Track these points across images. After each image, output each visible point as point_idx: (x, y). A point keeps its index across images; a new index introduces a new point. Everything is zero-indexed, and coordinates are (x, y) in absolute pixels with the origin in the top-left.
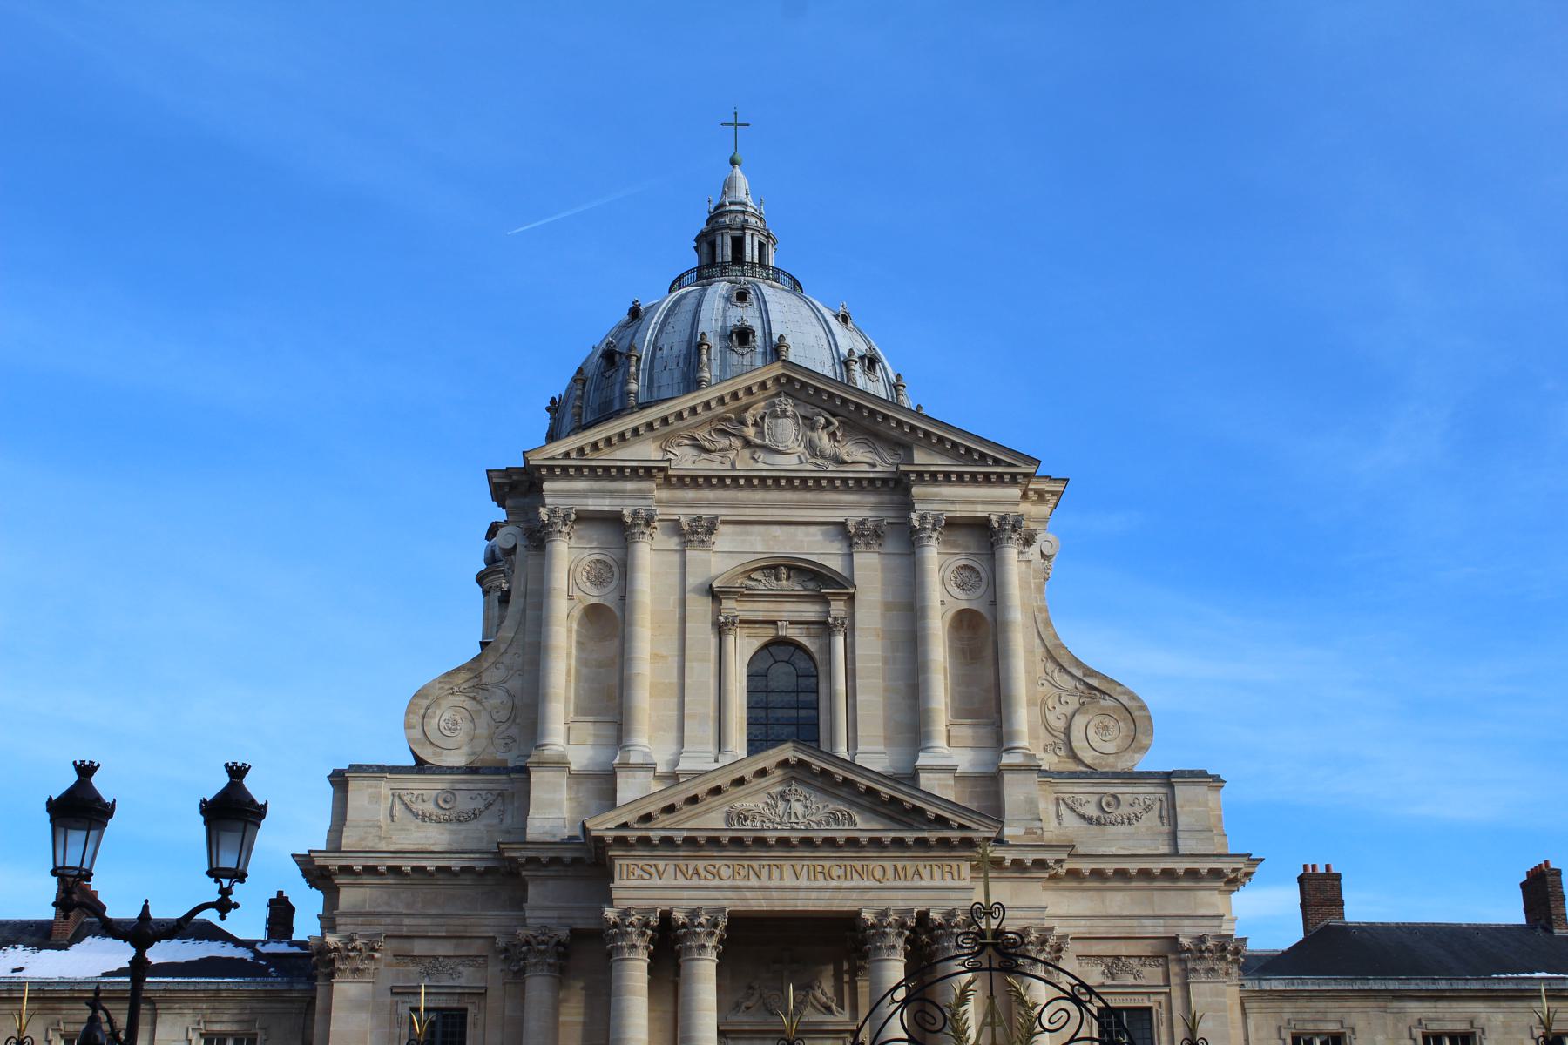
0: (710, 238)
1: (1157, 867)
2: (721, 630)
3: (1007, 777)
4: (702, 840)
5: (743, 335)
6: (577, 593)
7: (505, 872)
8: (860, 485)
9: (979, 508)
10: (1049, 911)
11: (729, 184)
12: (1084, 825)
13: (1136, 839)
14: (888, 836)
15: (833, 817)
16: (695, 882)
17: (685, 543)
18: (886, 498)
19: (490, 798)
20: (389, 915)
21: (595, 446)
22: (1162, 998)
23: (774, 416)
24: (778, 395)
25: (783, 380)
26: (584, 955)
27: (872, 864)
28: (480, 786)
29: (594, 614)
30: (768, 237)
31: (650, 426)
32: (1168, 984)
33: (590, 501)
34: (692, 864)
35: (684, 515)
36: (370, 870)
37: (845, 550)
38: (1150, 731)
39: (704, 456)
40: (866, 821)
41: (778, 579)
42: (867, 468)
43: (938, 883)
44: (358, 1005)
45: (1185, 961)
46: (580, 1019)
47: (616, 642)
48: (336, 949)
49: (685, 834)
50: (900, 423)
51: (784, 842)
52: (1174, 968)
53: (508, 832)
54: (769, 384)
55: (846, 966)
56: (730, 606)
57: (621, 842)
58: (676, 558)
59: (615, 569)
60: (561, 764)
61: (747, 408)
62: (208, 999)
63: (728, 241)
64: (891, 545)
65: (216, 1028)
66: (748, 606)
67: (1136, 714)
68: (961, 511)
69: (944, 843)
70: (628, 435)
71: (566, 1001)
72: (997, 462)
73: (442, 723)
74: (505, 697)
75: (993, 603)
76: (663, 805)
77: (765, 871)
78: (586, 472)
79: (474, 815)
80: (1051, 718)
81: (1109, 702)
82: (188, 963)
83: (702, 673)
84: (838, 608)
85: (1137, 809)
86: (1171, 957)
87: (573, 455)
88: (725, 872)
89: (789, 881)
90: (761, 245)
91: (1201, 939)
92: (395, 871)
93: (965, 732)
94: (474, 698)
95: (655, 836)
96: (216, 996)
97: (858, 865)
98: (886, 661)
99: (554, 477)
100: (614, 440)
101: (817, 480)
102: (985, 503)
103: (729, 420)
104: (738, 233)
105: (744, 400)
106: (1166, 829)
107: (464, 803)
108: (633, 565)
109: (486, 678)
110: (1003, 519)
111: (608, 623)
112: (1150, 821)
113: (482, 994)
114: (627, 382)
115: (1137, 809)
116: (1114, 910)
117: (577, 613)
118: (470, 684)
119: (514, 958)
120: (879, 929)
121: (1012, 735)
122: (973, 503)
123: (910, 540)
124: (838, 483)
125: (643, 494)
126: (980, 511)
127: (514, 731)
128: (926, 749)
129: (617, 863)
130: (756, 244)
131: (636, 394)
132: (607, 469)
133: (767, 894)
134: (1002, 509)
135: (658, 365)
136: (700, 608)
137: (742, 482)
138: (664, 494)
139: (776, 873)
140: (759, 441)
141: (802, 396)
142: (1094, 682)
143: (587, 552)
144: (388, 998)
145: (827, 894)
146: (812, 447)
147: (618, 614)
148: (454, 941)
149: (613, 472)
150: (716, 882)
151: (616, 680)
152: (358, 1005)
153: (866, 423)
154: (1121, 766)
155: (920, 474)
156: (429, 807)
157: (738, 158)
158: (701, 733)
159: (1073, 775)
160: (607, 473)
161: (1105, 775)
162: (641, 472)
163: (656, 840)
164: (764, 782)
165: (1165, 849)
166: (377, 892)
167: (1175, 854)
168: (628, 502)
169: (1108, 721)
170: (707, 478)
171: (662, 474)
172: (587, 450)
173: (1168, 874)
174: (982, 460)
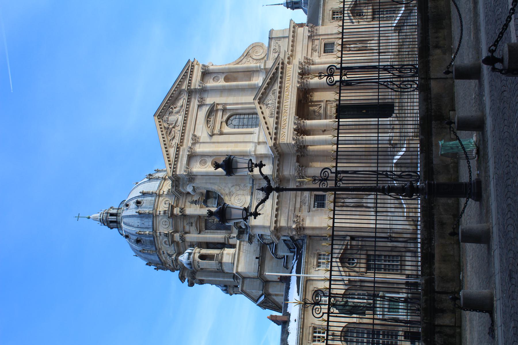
0: (109, 222)
2: (221, 134)
3: (267, 67)
5: (138, 203)
8: (189, 101)
11: (95, 219)
13: (284, 45)
14: (279, 80)
15: (273, 93)
16: (287, 125)
17: (198, 142)
18: (193, 96)
21: (169, 161)
30: (111, 208)
31: (166, 148)
32: (319, 39)
34: (282, 125)
36: (276, 216)
44: (312, 220)
45: (314, 36)
46: (319, 163)
50: (174, 91)
52: (315, 38)
56: (216, 131)
57: (275, 139)
58: (202, 145)
61: (165, 127)
64: (205, 96)
65: (315, 263)
66: (216, 128)
69: (282, 68)
72: (188, 69)
75: (223, 73)
81: (251, 52)
83: (232, 138)
84: (220, 107)
85: (277, 45)
88: (285, 118)
89: (289, 103)
91: (309, 31)
92: (277, 210)
93: (254, 79)
95: (274, 131)
96: (307, 263)
101: (186, 111)
102: (198, 73)
103: (167, 132)
104: (109, 214)
108: (202, 152)
109: (228, 192)
110: (202, 69)
112: (280, 43)
114: (146, 234)
121: (257, 67)
123: (203, 91)
125: (184, 150)
126: (200, 74)
127: (242, 185)
132: (176, 158)
134: (200, 68)
135: (143, 226)
136: (215, 138)
138: (184, 146)
141: (164, 114)
144: (311, 213)
145: (293, 95)
147: (214, 157)
152: (312, 220)
153: (173, 99)
154: (266, 49)
155: (188, 86)
157: (88, 216)
158: (247, 138)
159: (267, 58)
166: (282, 217)
170: (182, 136)
171: (179, 146)
173: (293, 37)
174: (188, 69)
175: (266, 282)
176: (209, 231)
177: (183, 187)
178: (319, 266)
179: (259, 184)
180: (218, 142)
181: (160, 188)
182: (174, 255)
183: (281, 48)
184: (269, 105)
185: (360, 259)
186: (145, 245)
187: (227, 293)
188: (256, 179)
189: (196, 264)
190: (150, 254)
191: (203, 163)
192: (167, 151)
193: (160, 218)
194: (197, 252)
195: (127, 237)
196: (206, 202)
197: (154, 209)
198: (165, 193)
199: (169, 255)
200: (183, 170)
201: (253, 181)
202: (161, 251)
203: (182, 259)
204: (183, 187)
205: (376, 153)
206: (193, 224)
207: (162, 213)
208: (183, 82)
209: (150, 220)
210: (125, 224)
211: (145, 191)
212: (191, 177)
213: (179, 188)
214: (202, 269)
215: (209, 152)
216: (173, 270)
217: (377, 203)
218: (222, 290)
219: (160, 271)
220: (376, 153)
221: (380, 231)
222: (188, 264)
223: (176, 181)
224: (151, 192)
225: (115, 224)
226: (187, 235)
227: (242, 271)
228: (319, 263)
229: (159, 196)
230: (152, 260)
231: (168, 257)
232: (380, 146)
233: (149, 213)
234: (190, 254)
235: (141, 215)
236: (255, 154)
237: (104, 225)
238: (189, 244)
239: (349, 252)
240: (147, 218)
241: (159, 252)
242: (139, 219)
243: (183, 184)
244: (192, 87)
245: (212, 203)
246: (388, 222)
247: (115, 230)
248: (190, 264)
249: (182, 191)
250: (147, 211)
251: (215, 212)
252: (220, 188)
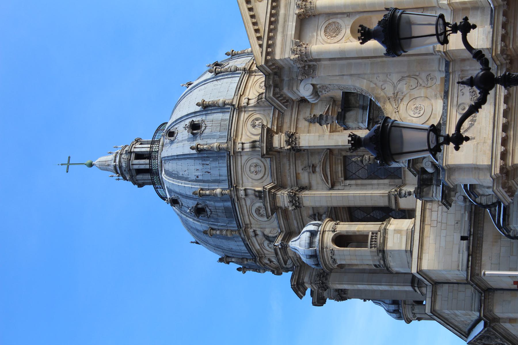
0: (134, 173)
5: (195, 127)
11: (104, 167)
21: (257, 31)
28: (456, 91)
30: (137, 141)
33: (289, 33)
36: (505, 142)
59: (331, 21)
63: (136, 162)
70: (252, 13)
73: (416, 115)
74: (404, 82)
78: (271, 34)
87: (261, 42)
90: (141, 144)
92: (505, 128)
94: (402, 100)
100: (254, 20)
104: (133, 156)
108: (330, 7)
109: (391, 94)
114: (215, 195)
127: (424, 75)
130: (141, 146)
131: (223, 189)
132: (271, 23)
135: (207, 177)
143: (319, 38)
157: (88, 162)
160: (273, 23)
168: (291, 12)
172: (258, 35)
175: (486, 292)
176: (353, 182)
177: (290, 88)
179: (462, 71)
181: (241, 91)
182: (280, 239)
186: (216, 219)
187: (400, 318)
188: (454, 61)
189: (327, 255)
190: (226, 238)
191: (333, 30)
192: (250, 9)
193: (244, 158)
194: (329, 229)
195: (174, 202)
196: (344, 118)
197: (229, 139)
198: (252, 102)
199: (267, 238)
200: (288, 50)
201: (447, 65)
202: (251, 231)
203: (297, 247)
204: (290, 88)
206: (317, 169)
207: (247, 146)
209: (223, 164)
210: (169, 174)
211: (208, 100)
212: (308, 65)
213: (281, 89)
214: (341, 266)
215: (345, 6)
216: (277, 271)
218: (388, 311)
219: (249, 273)
222: (311, 257)
223: (275, 74)
224: (221, 102)
225: (148, 177)
226: (305, 194)
227: (431, 268)
229: (240, 109)
230: (231, 250)
231: (266, 243)
233: (220, 149)
234: (313, 234)
235: (202, 154)
236: (449, 4)
237: (125, 179)
238: (311, 212)
240: (215, 159)
241: (246, 231)
242: (198, 162)
243: (291, 80)
245: (356, 120)
247: (149, 189)
248: (313, 256)
249: (290, 95)
250: (215, 143)
251: (365, 138)
252: (372, 85)
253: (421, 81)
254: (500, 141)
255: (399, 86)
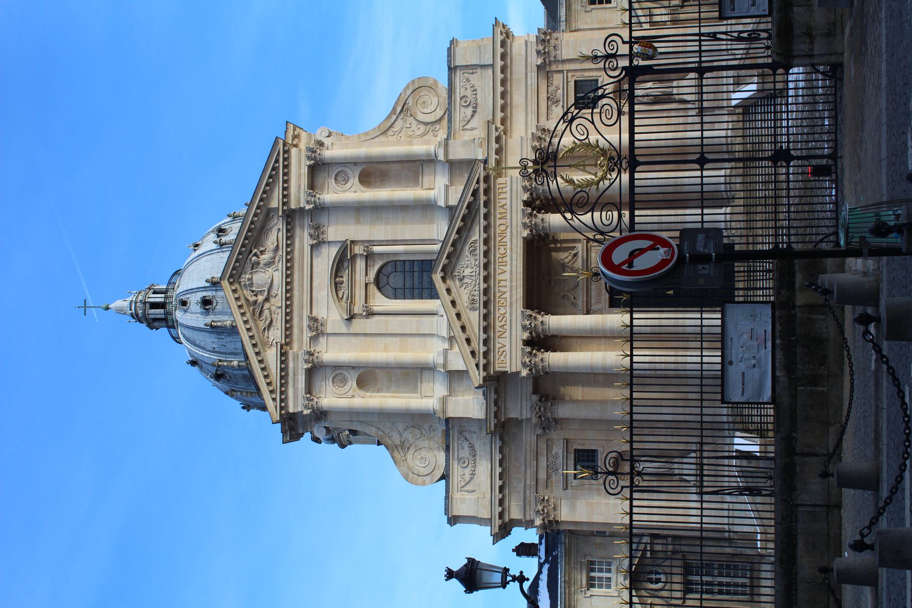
0: (151, 321)
1: (499, 76)
2: (370, 314)
3: (451, 157)
4: (485, 323)
6: (350, 393)
7: (502, 430)
8: (290, 237)
9: (302, 171)
10: (523, 135)
11: (120, 311)
12: (476, 115)
13: (484, 86)
14: (483, 223)
16: (507, 327)
17: (323, 334)
18: (297, 223)
19: (462, 438)
20: (525, 492)
21: (269, 384)
22: (570, 75)
23: (252, 285)
24: (240, 283)
25: (231, 280)
26: (546, 387)
27: (498, 231)
29: (362, 383)
30: (150, 289)
31: (257, 354)
32: (563, 71)
33: (300, 386)
34: (498, 329)
35: (307, 334)
37: (326, 245)
38: (426, 78)
39: (274, 324)
40: (474, 234)
41: (342, 283)
42: (280, 234)
43: (508, 195)
44: (573, 507)
45: (550, 62)
46: (580, 388)
47: (377, 371)
48: (543, 520)
49: (482, 333)
50: (255, 215)
51: (486, 279)
52: (554, 68)
53: (481, 428)
54: (233, 288)
55: (552, 246)
56: (357, 309)
57: (486, 367)
58: (331, 338)
59: (337, 372)
60: (444, 401)
61: (247, 300)
62: (569, 587)
63: (152, 311)
64: (324, 220)
65: (584, 582)
66: (357, 299)
67: (416, 86)
68: (304, 181)
69: (487, 192)
70: (263, 366)
71: (570, 397)
72: (277, 161)
74: (407, 432)
75: (355, 164)
76: (466, 345)
77: (502, 289)
78: (283, 389)
79: (472, 447)
80: (418, 133)
81: (410, 101)
82: (550, 598)
84: (358, 250)
85: (468, 86)
86: (548, 69)
87: (274, 396)
88: (502, 311)
89: (507, 276)
90: (154, 293)
91: (538, 52)
93: (426, 180)
95: (483, 349)
96: (568, 583)
97: (498, 239)
98: (387, 223)
99: (286, 406)
100: (266, 373)
101: (288, 261)
102: (300, 168)
103: (254, 310)
104: (148, 306)
105: (243, 301)
106: (479, 70)
107: (465, 453)
109: (397, 442)
110: (309, 158)
111: (366, 375)
112: (475, 79)
113: (567, 441)
114: (233, 367)
115: (468, 86)
116: (523, 100)
117: (362, 393)
118: (400, 450)
119: (548, 424)
120: (532, 228)
121: (429, 155)
122: (300, 175)
123: (320, 209)
124: (289, 250)
125: (296, 357)
126: (305, 171)
128: (436, 202)
129: (497, 369)
131: (239, 362)
133: (514, 288)
135: (223, 350)
136: (359, 325)
137: (288, 303)
138: (295, 345)
139: (502, 283)
140: (266, 293)
141: (240, 270)
142: (399, 109)
144: (569, 491)
145: (514, 256)
146: (269, 264)
147: (362, 370)
148: (539, 457)
149: (283, 374)
150: (508, 315)
151: (398, 371)
152: (573, 507)
154: (445, 95)
155: (284, 204)
156: (468, 471)
157: (104, 306)
159: (450, 121)
160: (284, 377)
161: (450, 103)
162: (283, 358)
163: (485, 349)
164: (453, 290)
165: (490, 71)
166: (513, 499)
167: (492, 66)
168: (300, 366)
169: (420, 101)
172: (271, 388)
173: (503, 70)
174: (276, 169)
178: (593, 586)
180: (365, 335)
183: (479, 92)
184: (466, 280)
185: (671, 574)
205: (698, 381)
208: (272, 190)
217: (702, 458)
220: (698, 381)
221: (709, 426)
228: (593, 579)
232: (705, 520)
239: (647, 561)
244: (293, 206)
246: (726, 513)
253: (424, 432)
254: (497, 502)
255: (405, 435)
